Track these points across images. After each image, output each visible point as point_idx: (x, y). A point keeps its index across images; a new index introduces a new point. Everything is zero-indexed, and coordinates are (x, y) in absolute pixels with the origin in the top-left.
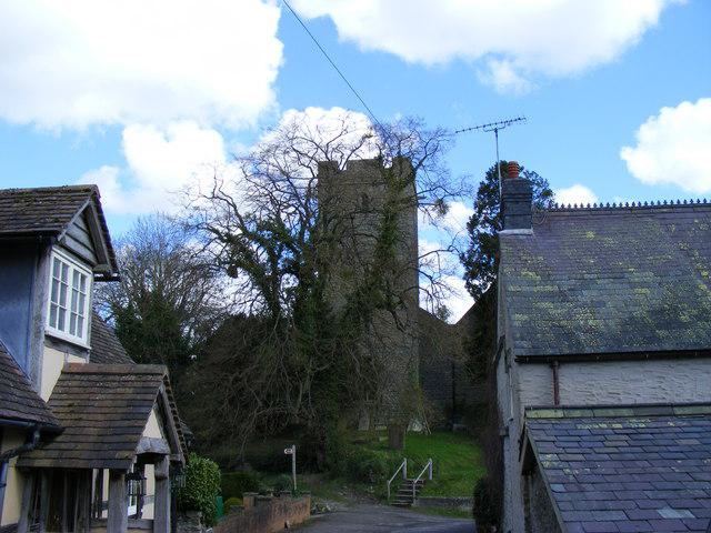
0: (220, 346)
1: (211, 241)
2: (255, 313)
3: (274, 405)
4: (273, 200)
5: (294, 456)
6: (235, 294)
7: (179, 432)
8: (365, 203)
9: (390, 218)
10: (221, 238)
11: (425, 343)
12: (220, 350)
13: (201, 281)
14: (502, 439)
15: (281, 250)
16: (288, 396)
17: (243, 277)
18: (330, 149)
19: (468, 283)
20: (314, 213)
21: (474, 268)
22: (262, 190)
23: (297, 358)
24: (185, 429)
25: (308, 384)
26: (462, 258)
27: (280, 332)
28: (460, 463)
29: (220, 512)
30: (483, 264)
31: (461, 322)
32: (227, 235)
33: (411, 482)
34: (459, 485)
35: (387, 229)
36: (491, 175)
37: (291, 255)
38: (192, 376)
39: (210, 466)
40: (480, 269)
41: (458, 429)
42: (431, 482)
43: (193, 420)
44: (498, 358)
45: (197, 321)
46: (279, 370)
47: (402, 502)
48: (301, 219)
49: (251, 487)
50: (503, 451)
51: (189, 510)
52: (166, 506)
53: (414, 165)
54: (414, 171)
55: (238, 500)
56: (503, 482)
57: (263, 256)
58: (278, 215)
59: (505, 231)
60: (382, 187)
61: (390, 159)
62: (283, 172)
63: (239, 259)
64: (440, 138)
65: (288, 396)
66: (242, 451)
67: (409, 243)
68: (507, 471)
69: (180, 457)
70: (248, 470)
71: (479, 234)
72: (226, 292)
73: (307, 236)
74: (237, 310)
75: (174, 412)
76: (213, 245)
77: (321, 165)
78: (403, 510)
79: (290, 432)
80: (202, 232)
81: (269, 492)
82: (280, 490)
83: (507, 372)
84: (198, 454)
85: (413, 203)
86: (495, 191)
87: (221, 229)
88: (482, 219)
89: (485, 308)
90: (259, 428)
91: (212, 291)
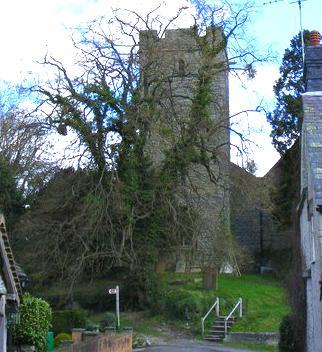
0: (51, 197)
1: (43, 102)
2: (83, 167)
3: (99, 250)
4: (98, 65)
5: (118, 295)
6: (64, 151)
7: (14, 275)
8: (182, 68)
9: (204, 81)
10: (52, 99)
11: (236, 195)
12: (51, 200)
13: (34, 138)
14: (305, 280)
15: (106, 110)
16: (112, 241)
17: (72, 134)
18: (150, 20)
19: (274, 140)
20: (136, 77)
21: (279, 126)
22: (90, 56)
23: (121, 207)
24: (20, 271)
25: (130, 231)
26: (269, 117)
27: (105, 184)
28: (267, 302)
29: (51, 345)
30: (288, 123)
31: (268, 175)
32: (57, 96)
33: (223, 319)
34: (266, 322)
35: (201, 92)
36: (295, 43)
37: (115, 115)
38: (27, 224)
39: (42, 305)
40: (286, 128)
41: (265, 271)
42: (241, 319)
43: (27, 263)
44: (302, 207)
45: (30, 174)
46: (104, 218)
47: (215, 337)
48: (124, 83)
49: (77, 323)
50: (306, 291)
51: (24, 344)
52: (2, 340)
53: (226, 34)
54: (225, 39)
55: (68, 336)
56: (305, 318)
57: (90, 117)
58: (103, 79)
59: (308, 93)
60: (197, 53)
61: (204, 28)
62: (108, 40)
63: (69, 119)
64: (249, 10)
65: (112, 241)
66: (70, 291)
67: (221, 104)
68: (309, 309)
69: (15, 297)
70: (76, 308)
71: (285, 96)
72: (56, 149)
73: (129, 97)
74: (65, 165)
75: (9, 256)
76: (45, 104)
77: (142, 34)
78: (215, 344)
79: (114, 274)
80: (35, 94)
81: (95, 328)
82: (105, 326)
83: (309, 220)
84: (31, 293)
85: (224, 68)
86: (298, 57)
87: (51, 92)
88: (287, 82)
89: (289, 162)
90: (87, 271)
91: (43, 147)
